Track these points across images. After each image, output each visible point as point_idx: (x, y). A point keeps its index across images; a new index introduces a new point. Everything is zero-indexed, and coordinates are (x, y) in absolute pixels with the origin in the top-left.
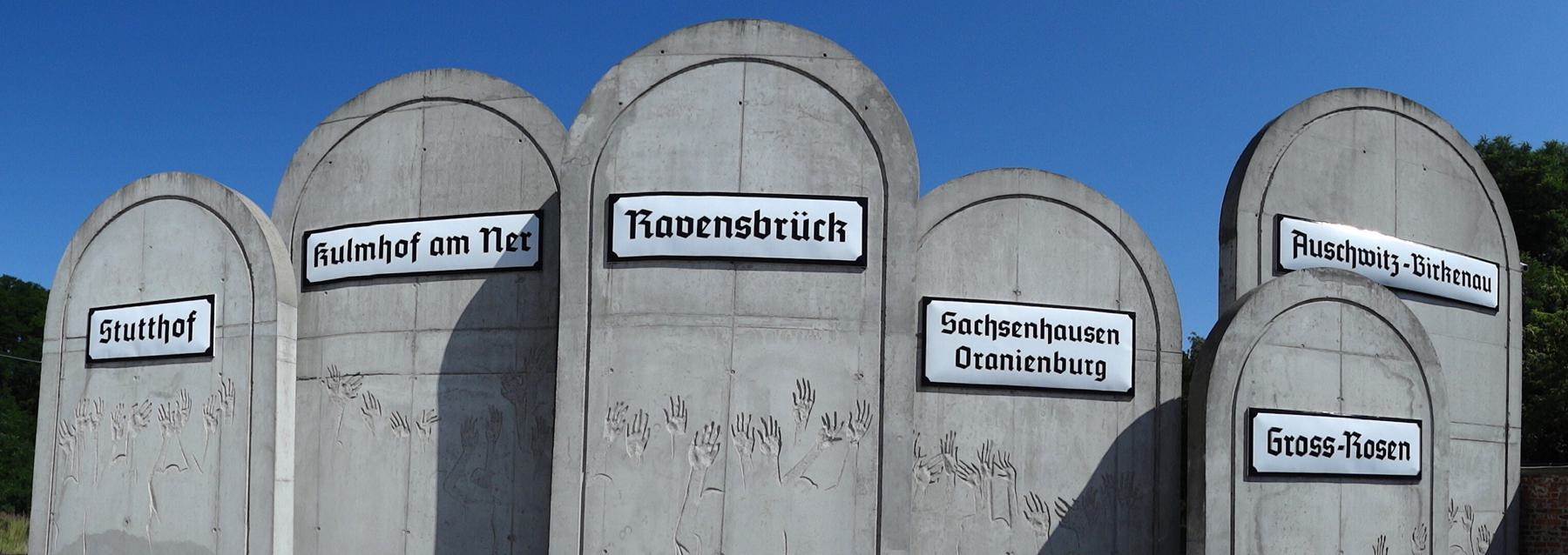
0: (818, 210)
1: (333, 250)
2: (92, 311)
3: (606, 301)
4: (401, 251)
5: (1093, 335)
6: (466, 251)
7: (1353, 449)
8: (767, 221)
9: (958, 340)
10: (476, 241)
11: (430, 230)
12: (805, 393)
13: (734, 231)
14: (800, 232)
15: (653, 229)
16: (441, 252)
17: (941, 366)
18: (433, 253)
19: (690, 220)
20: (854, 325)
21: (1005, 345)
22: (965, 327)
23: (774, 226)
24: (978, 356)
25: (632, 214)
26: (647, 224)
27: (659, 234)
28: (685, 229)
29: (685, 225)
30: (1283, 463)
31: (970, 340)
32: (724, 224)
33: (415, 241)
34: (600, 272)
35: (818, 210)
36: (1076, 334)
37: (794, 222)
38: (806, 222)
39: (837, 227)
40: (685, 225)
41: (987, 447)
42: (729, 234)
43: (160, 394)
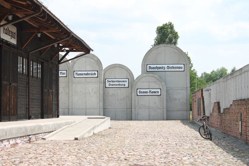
0: (93, 72)
3: (74, 81)
5: (123, 81)
12: (92, 90)
17: (107, 85)
20: (97, 83)
22: (110, 82)
23: (89, 74)
31: (110, 83)
34: (73, 78)
35: (93, 72)
41: (112, 93)
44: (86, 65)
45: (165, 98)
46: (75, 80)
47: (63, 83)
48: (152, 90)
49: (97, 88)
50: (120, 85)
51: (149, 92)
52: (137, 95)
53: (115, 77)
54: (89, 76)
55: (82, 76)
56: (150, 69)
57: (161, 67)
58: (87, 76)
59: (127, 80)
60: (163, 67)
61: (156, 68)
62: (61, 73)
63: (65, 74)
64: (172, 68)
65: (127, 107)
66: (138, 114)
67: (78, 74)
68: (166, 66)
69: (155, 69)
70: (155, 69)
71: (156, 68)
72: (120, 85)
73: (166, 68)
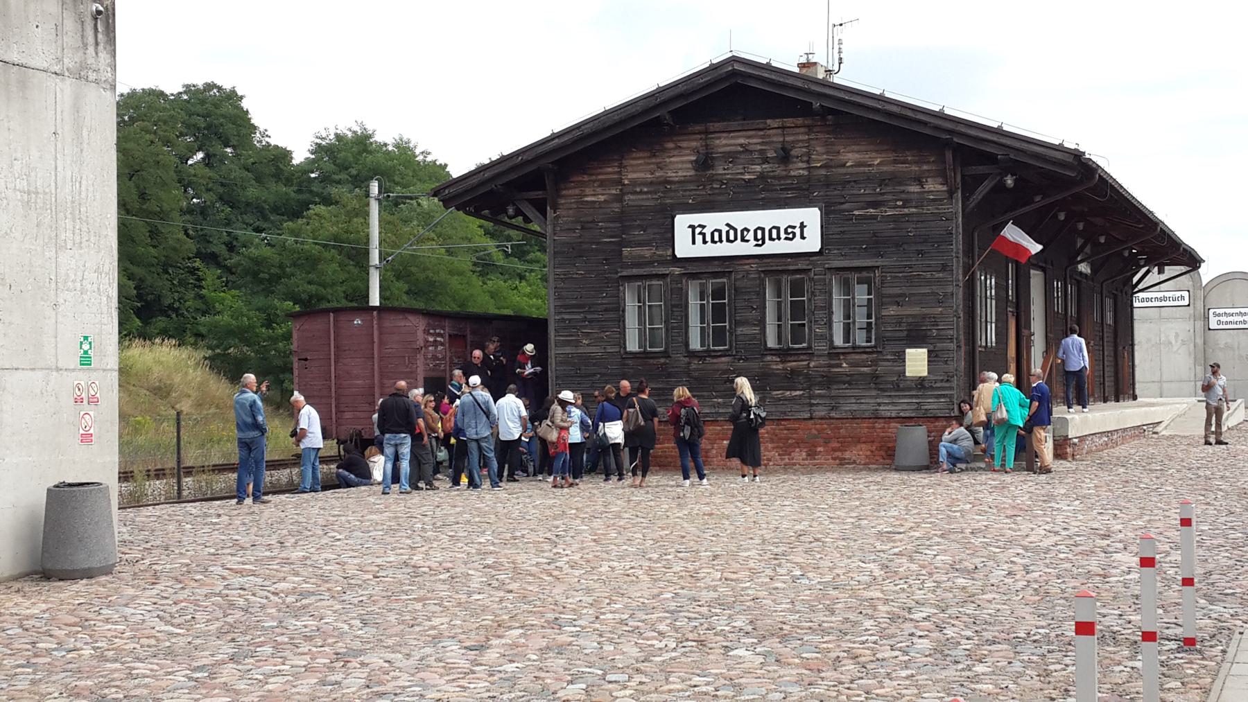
12: (1177, 335)
21: (1231, 319)
22: (1219, 315)
55: (1150, 304)
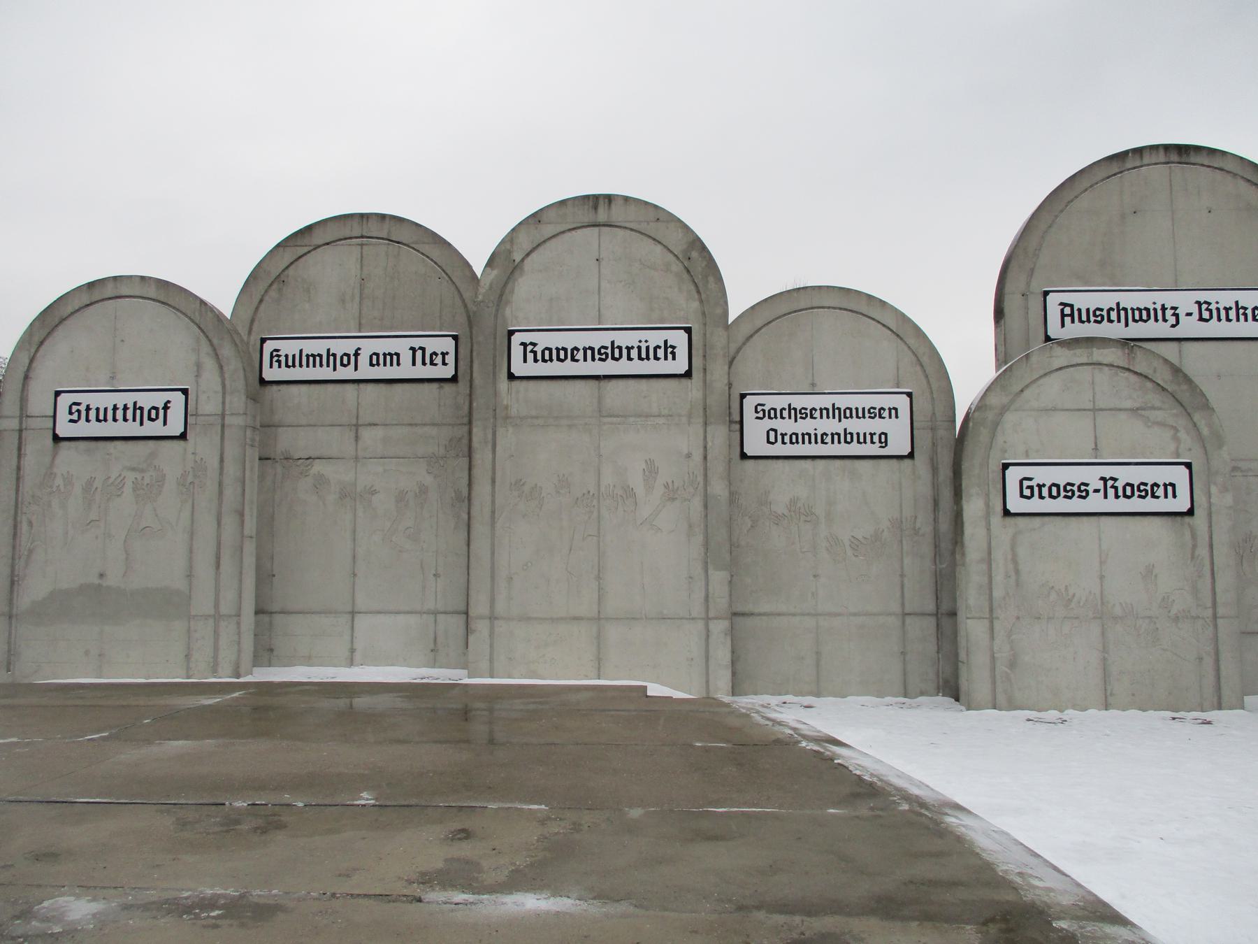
0: (656, 338)
1: (287, 356)
2: (58, 394)
3: (506, 407)
4: (345, 362)
6: (398, 364)
7: (1111, 492)
8: (620, 348)
9: (768, 424)
10: (406, 357)
11: (368, 347)
12: (651, 471)
13: (597, 356)
14: (644, 355)
15: (539, 357)
16: (378, 364)
17: (755, 443)
18: (372, 365)
19: (565, 349)
20: (684, 419)
22: (773, 414)
23: (625, 352)
24: (783, 435)
25: (524, 345)
26: (535, 353)
27: (544, 360)
28: (562, 356)
29: (562, 353)
30: (1035, 505)
32: (591, 353)
33: (356, 354)
35: (656, 338)
36: (860, 414)
37: (639, 348)
38: (648, 348)
39: (670, 350)
40: (562, 353)
41: (793, 501)
42: (593, 359)
43: (133, 469)
44: (604, 284)
45: (1222, 538)
46: (513, 398)
47: (434, 424)
48: (1125, 475)
49: (689, 456)
50: (848, 437)
51: (1097, 491)
52: (1007, 513)
53: (813, 385)
54: (623, 367)
55: (568, 368)
56: (1068, 320)
57: (1151, 307)
58: (610, 367)
59: (902, 403)
60: (1164, 308)
61: (1114, 315)
62: (419, 353)
63: (444, 364)
64: (1232, 314)
65: (903, 605)
66: (1012, 664)
67: (539, 349)
68: (1185, 301)
69: (1110, 321)
70: (1110, 321)
71: (1114, 315)
72: (848, 437)
73: (1189, 314)
